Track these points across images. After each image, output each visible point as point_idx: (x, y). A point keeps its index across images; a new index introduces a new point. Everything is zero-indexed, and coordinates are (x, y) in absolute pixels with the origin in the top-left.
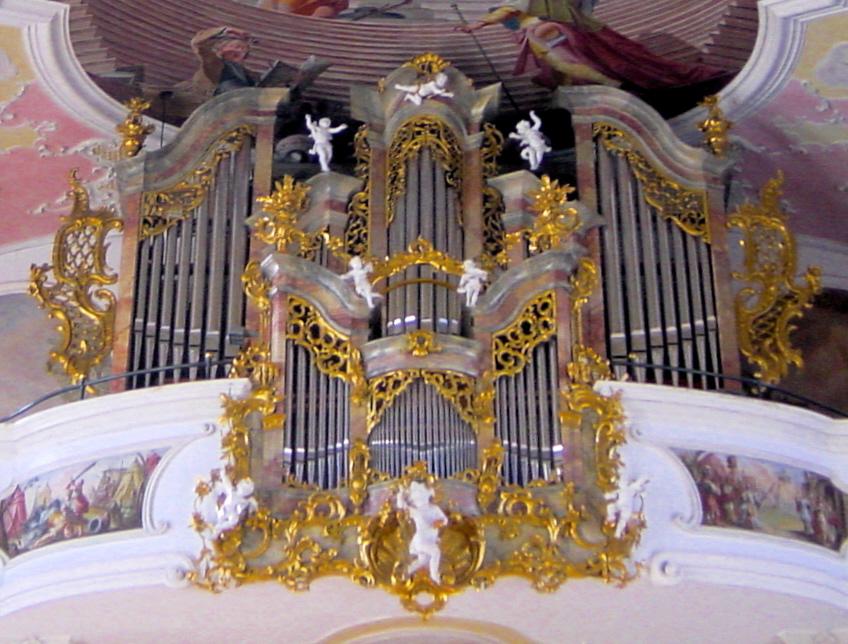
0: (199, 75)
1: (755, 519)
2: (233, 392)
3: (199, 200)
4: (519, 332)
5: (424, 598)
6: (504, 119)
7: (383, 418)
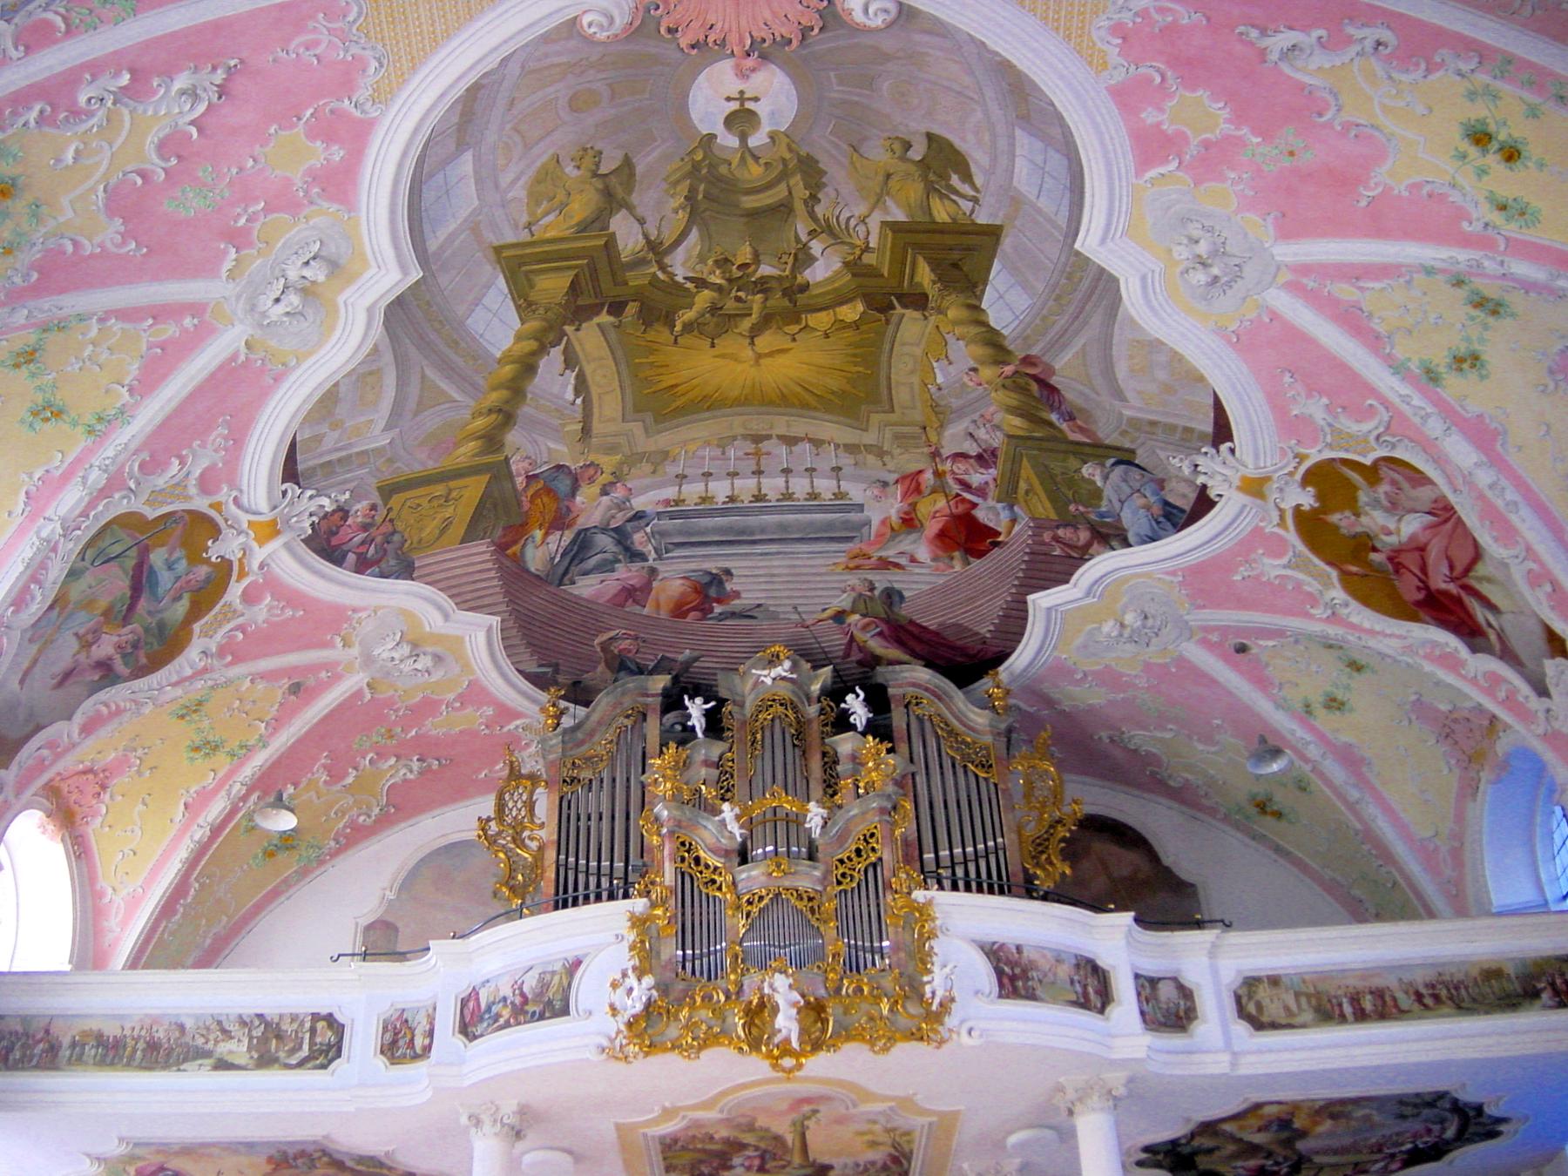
0: (601, 668)
1: (1038, 992)
3: (605, 763)
4: (853, 856)
5: (788, 1062)
6: (836, 693)
7: (752, 925)
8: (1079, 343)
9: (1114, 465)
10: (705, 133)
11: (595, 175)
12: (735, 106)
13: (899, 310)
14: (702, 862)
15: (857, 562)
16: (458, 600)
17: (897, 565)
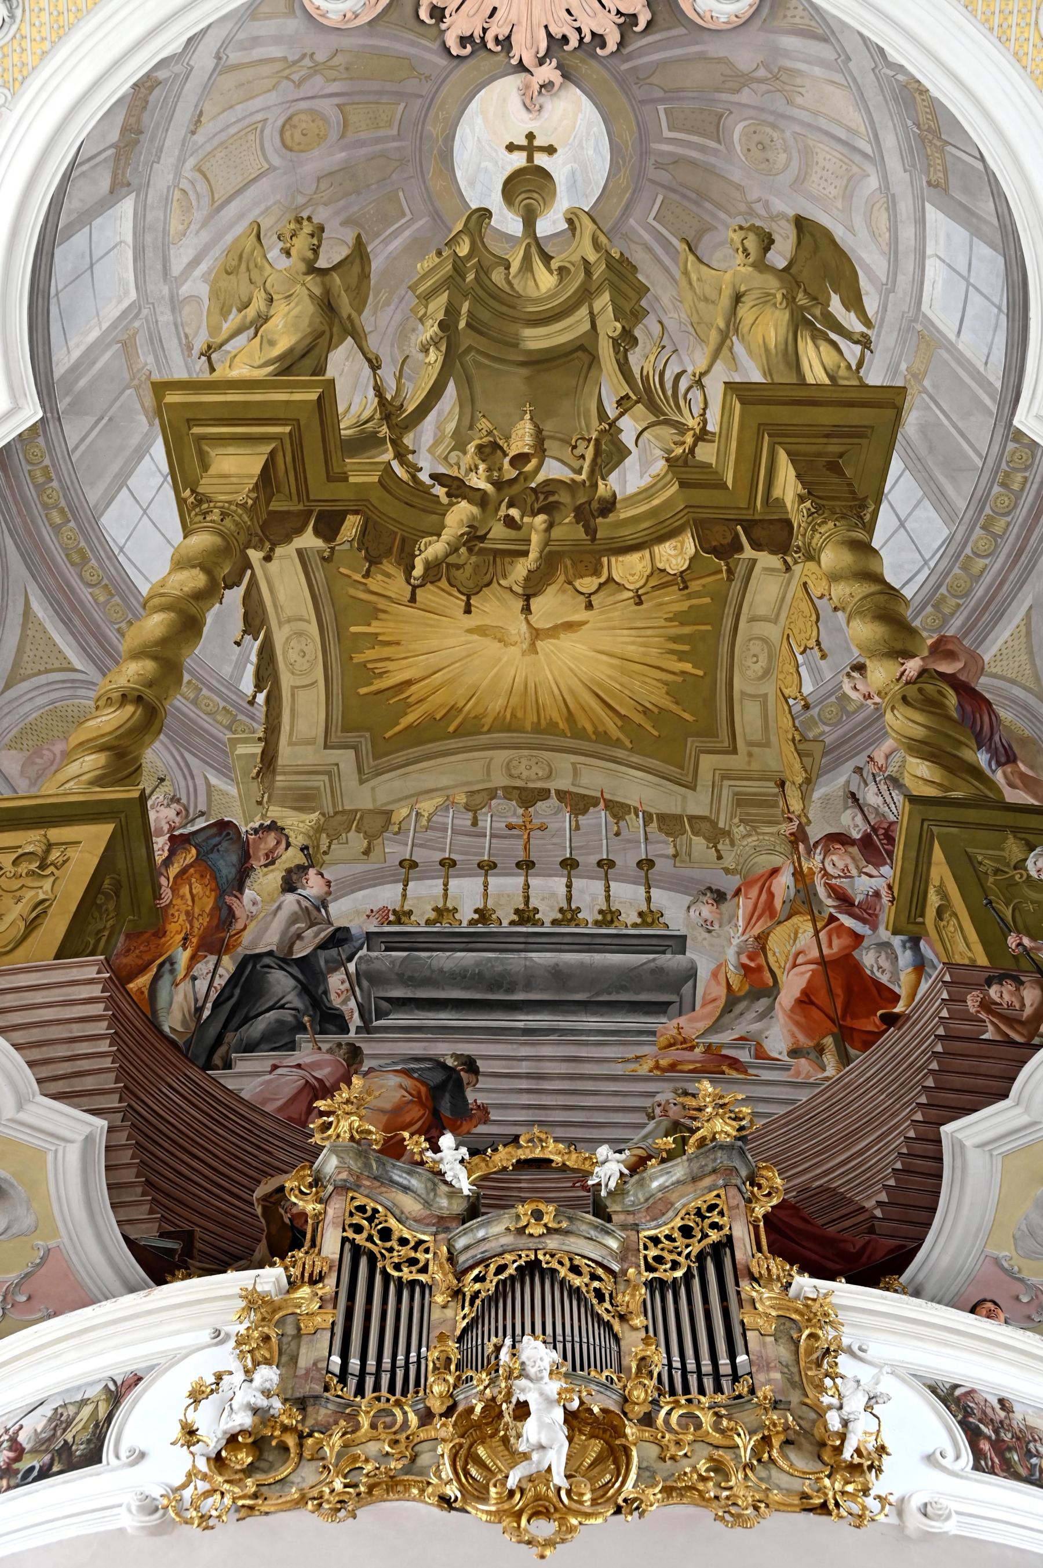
2: (259, 1288)
4: (676, 1235)
10: (474, 206)
11: (312, 269)
12: (519, 160)
13: (749, 552)
14: (395, 1236)
15: (674, 1055)
16: (46, 1071)
17: (735, 1064)
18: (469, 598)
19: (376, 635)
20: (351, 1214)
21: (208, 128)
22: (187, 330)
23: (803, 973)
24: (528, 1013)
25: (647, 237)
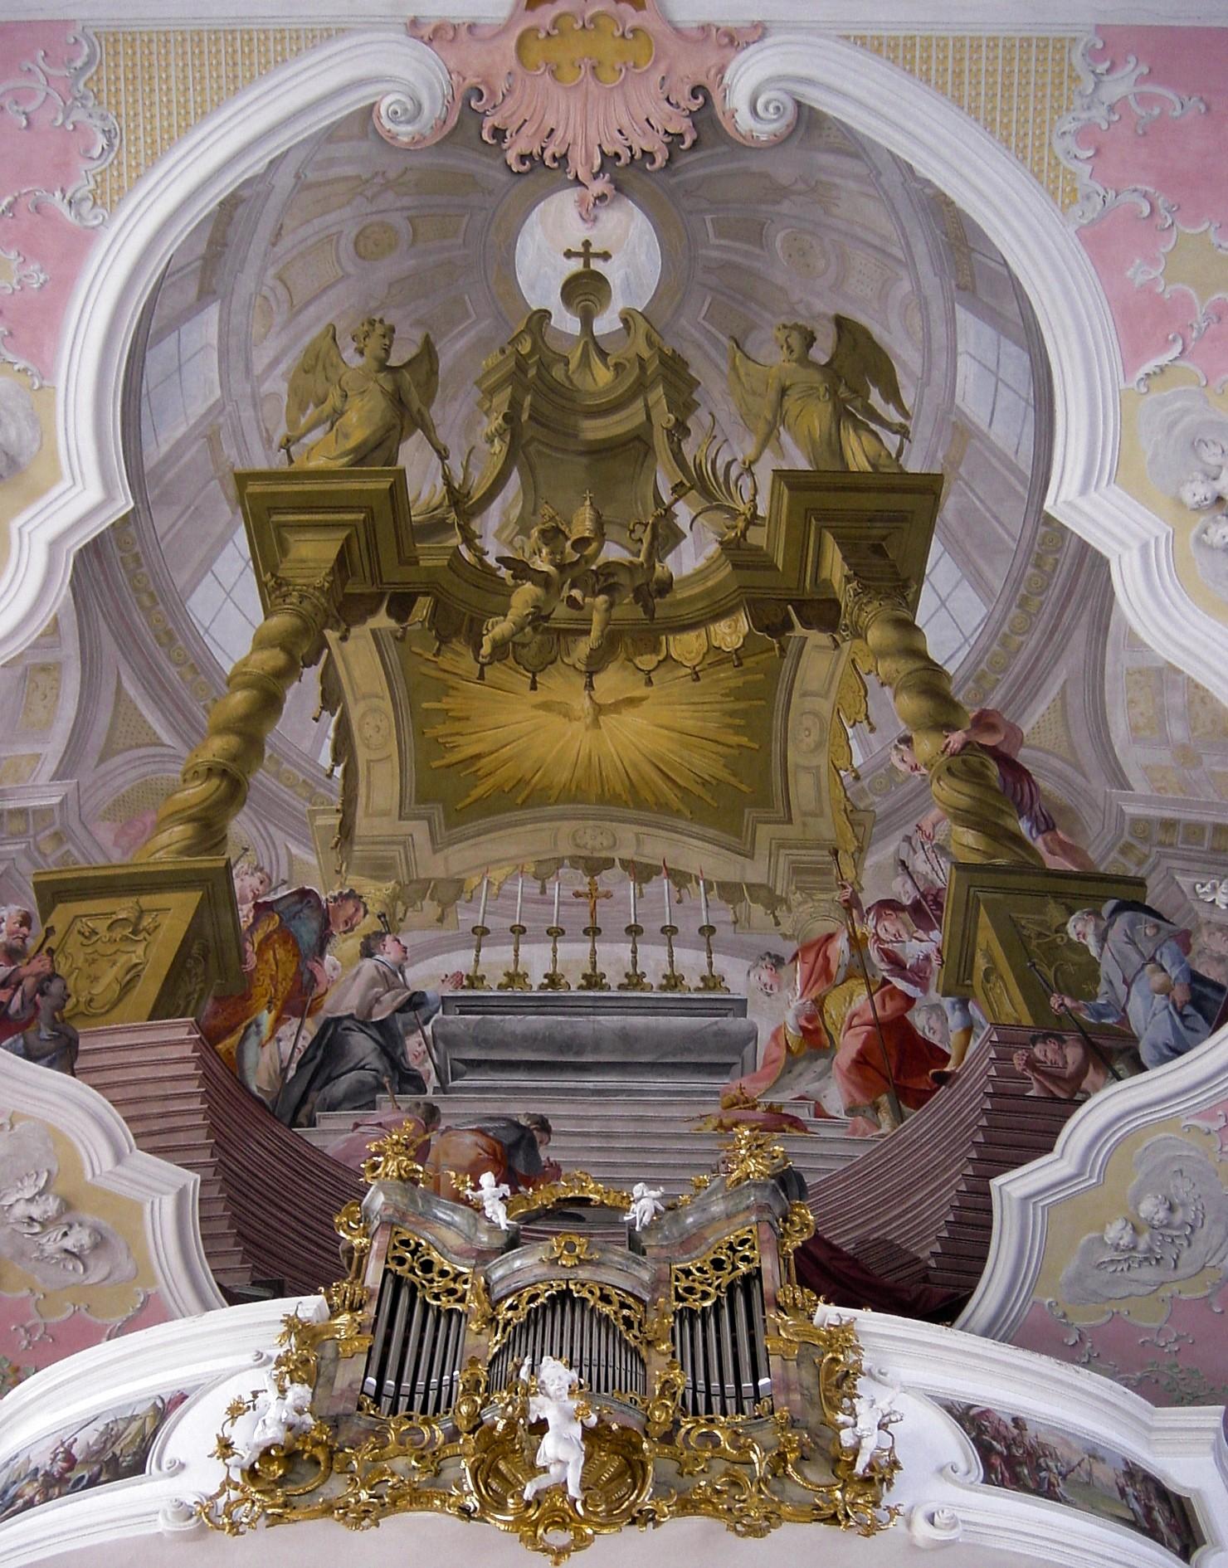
2: (300, 1315)
8: (1053, 689)
9: (1116, 911)
10: (535, 308)
11: (383, 367)
12: (576, 265)
13: (799, 630)
14: (436, 1269)
16: (141, 1127)
17: (795, 1123)
18: (534, 677)
19: (447, 711)
20: (395, 1247)
21: (287, 241)
22: (268, 426)
23: (857, 1035)
24: (597, 1074)
25: (697, 335)
